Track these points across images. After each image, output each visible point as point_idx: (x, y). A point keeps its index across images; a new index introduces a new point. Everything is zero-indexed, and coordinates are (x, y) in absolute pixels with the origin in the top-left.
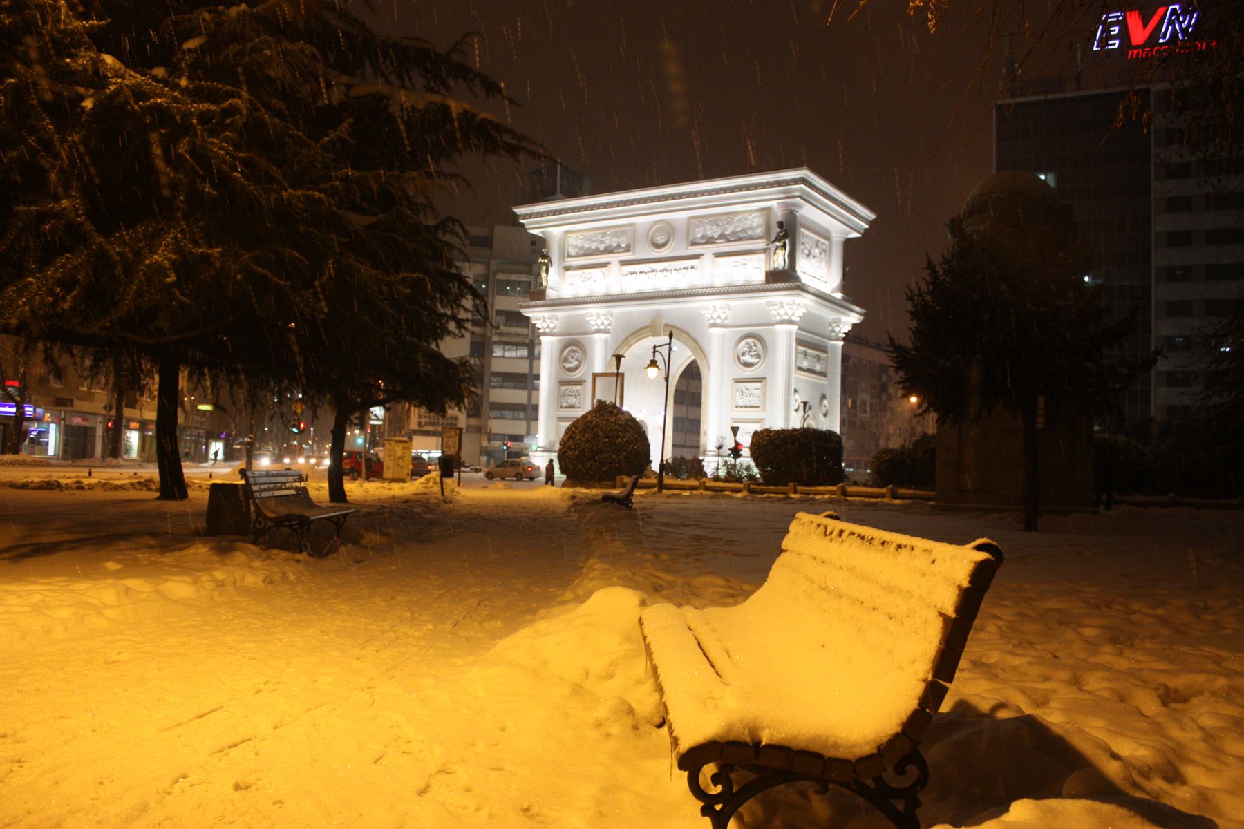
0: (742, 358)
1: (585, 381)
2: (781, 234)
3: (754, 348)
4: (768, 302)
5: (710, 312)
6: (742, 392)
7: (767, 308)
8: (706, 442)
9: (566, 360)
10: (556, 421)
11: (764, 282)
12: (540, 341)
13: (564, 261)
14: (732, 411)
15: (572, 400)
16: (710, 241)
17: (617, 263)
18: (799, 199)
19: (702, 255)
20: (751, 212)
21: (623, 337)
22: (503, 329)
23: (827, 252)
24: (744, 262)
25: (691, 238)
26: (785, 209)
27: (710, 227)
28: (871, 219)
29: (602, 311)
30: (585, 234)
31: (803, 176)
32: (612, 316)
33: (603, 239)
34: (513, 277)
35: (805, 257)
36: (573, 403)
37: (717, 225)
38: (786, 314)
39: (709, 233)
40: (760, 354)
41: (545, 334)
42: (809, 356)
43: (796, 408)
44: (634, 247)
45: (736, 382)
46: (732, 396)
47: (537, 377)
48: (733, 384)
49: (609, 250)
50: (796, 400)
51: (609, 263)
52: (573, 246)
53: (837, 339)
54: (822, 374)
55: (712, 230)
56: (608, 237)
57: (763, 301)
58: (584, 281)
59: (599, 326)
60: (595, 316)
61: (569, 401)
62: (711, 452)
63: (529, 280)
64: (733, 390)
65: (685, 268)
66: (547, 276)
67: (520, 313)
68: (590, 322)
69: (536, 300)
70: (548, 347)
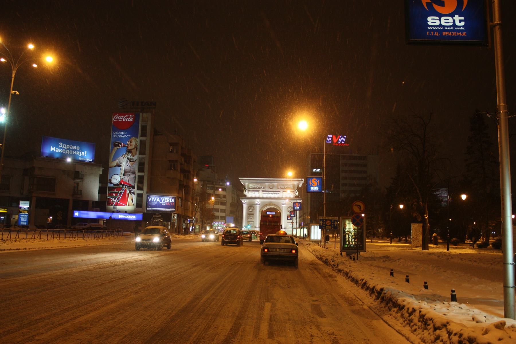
9: (249, 209)
15: (252, 218)
16: (282, 189)
20: (290, 184)
21: (263, 206)
39: (281, 187)
41: (244, 204)
49: (259, 188)
60: (257, 201)
70: (245, 207)
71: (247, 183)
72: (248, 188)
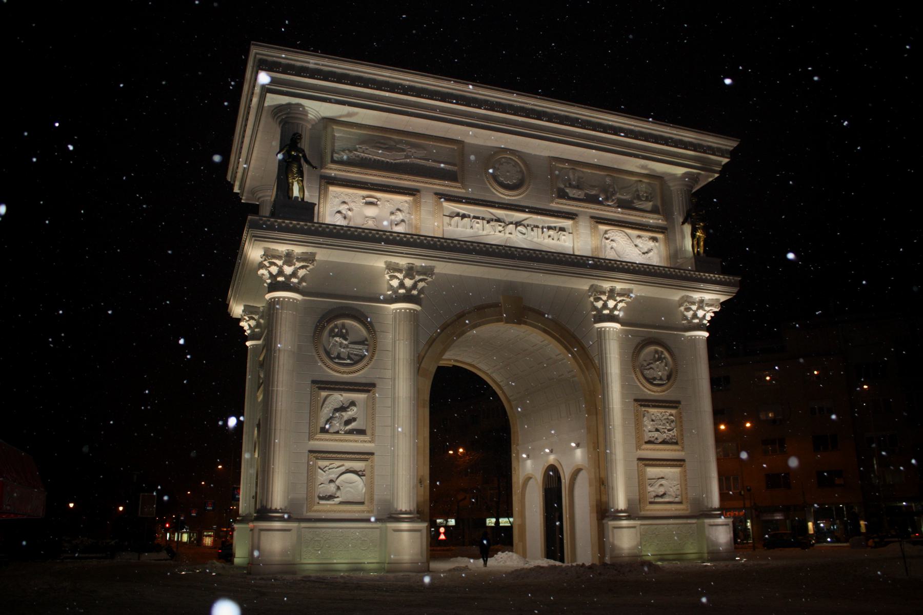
1: (373, 385)
2: (701, 213)
4: (688, 297)
5: (604, 298)
11: (694, 269)
13: (323, 166)
19: (576, 215)
62: (622, 511)
65: (549, 228)
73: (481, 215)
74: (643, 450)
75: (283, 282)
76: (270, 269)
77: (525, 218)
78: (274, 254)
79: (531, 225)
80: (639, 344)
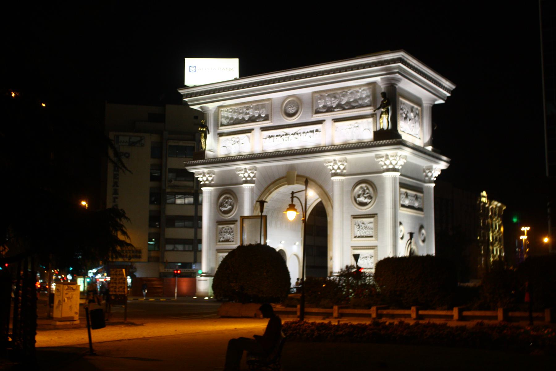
0: (358, 199)
1: (236, 221)
2: (385, 102)
3: (367, 191)
4: (376, 155)
5: (332, 164)
6: (359, 225)
7: (375, 159)
8: (332, 265)
9: (222, 205)
10: (215, 252)
12: (202, 190)
13: (218, 129)
14: (351, 240)
15: (228, 236)
16: (329, 109)
17: (259, 129)
18: (397, 74)
19: (324, 121)
20: (360, 86)
21: (266, 186)
22: (173, 182)
23: (419, 116)
24: (356, 125)
25: (315, 108)
26: (386, 83)
27: (329, 99)
28: (452, 89)
29: (248, 166)
30: (233, 108)
31: (401, 56)
32: (256, 170)
33: (248, 111)
34: (181, 143)
35: (403, 119)
36: (229, 238)
37: (335, 97)
38: (391, 163)
39: (329, 104)
40: (372, 195)
41: (205, 185)
42: (409, 195)
43: (401, 236)
44: (271, 115)
45: (354, 218)
46: (351, 229)
47: (200, 218)
48: (351, 220)
49: (252, 120)
50: (401, 231)
51: (253, 129)
52: (224, 117)
53: (430, 182)
54: (420, 209)
55: (331, 101)
56: (251, 110)
57: (373, 154)
58: (234, 144)
59: (246, 178)
61: (225, 236)
63: (193, 145)
64: (351, 224)
65: (311, 132)
66: (205, 141)
67: (186, 170)
68: (240, 175)
69: (197, 160)
71: (212, 107)
72: (218, 123)
73: (278, 134)
74: (353, 241)
75: (203, 184)
76: (203, 178)
77: (298, 130)
78: (198, 173)
79: (301, 133)
80: (354, 185)
